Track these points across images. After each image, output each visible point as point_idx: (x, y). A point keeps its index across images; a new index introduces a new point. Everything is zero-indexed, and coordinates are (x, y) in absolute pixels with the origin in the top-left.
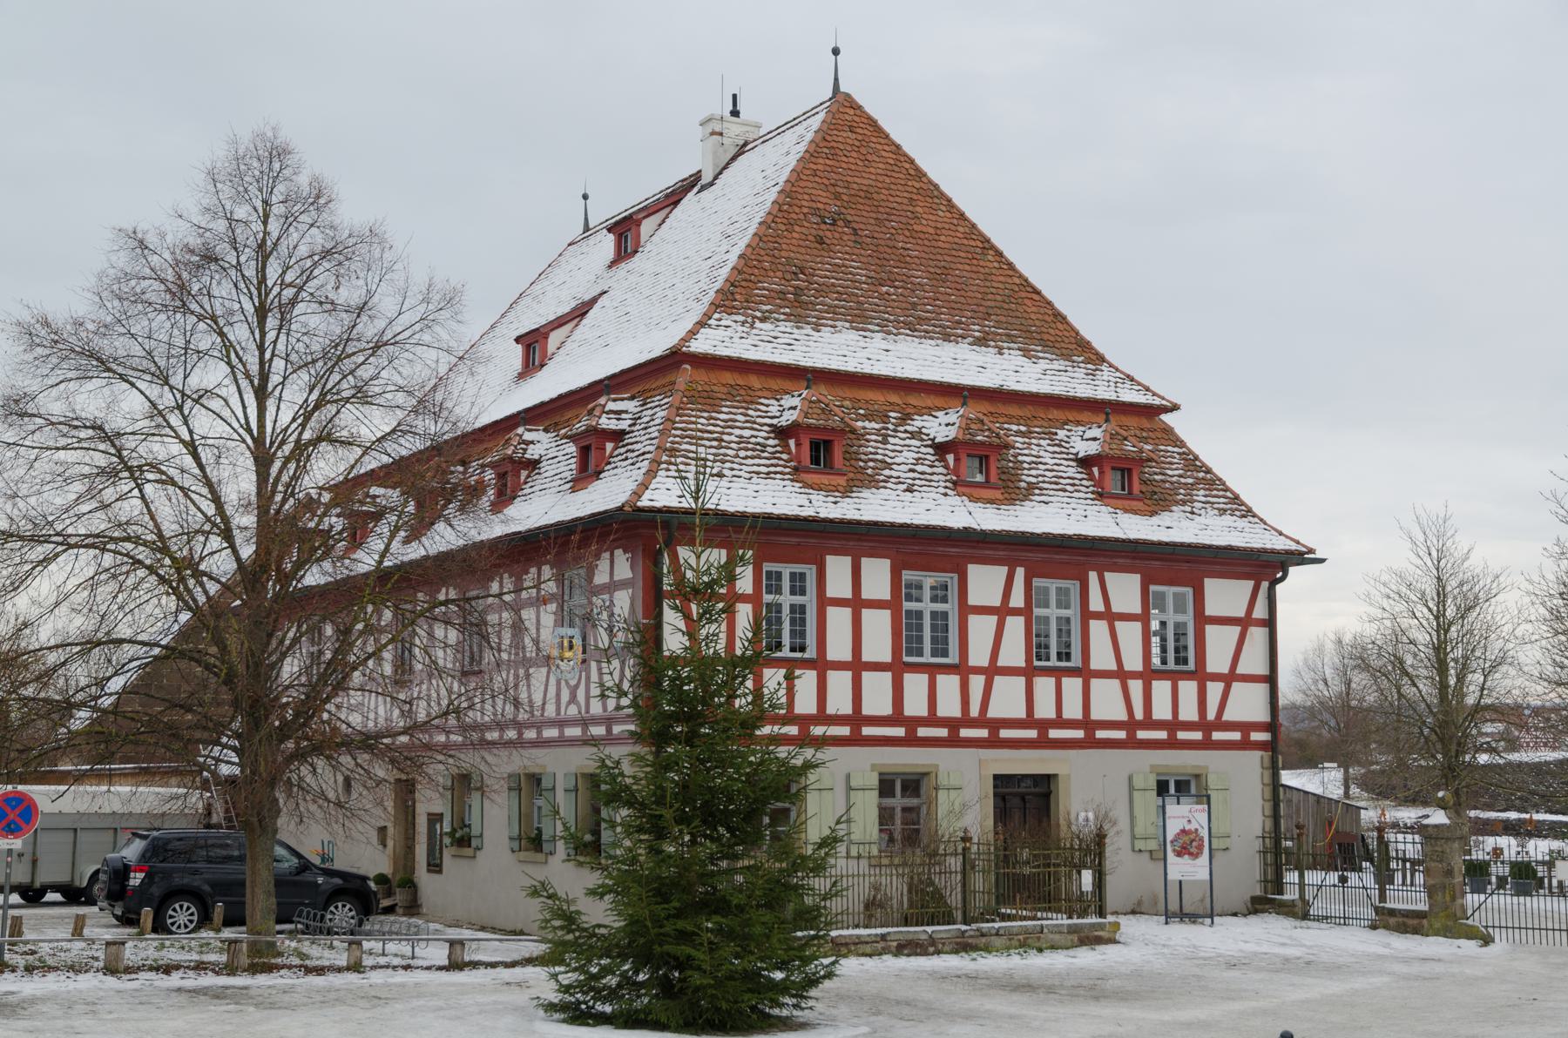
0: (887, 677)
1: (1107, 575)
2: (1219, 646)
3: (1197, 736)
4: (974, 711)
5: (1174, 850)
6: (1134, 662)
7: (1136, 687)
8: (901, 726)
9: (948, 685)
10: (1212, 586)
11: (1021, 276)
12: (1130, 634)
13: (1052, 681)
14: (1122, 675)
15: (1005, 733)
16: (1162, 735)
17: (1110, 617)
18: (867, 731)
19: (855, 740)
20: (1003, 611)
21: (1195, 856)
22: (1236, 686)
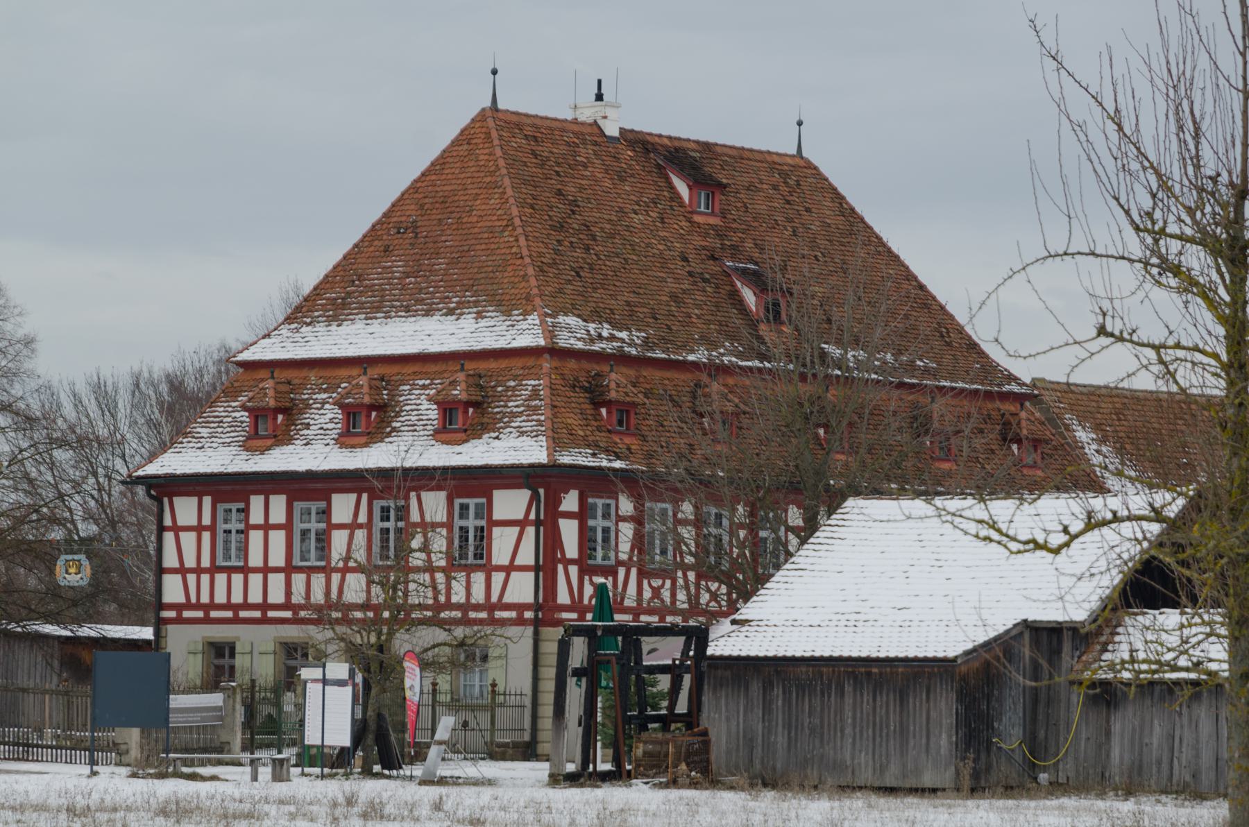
0: (282, 576)
3: (483, 615)
9: (318, 581)
10: (500, 497)
17: (266, 527)
18: (271, 614)
19: (264, 620)
20: (353, 527)
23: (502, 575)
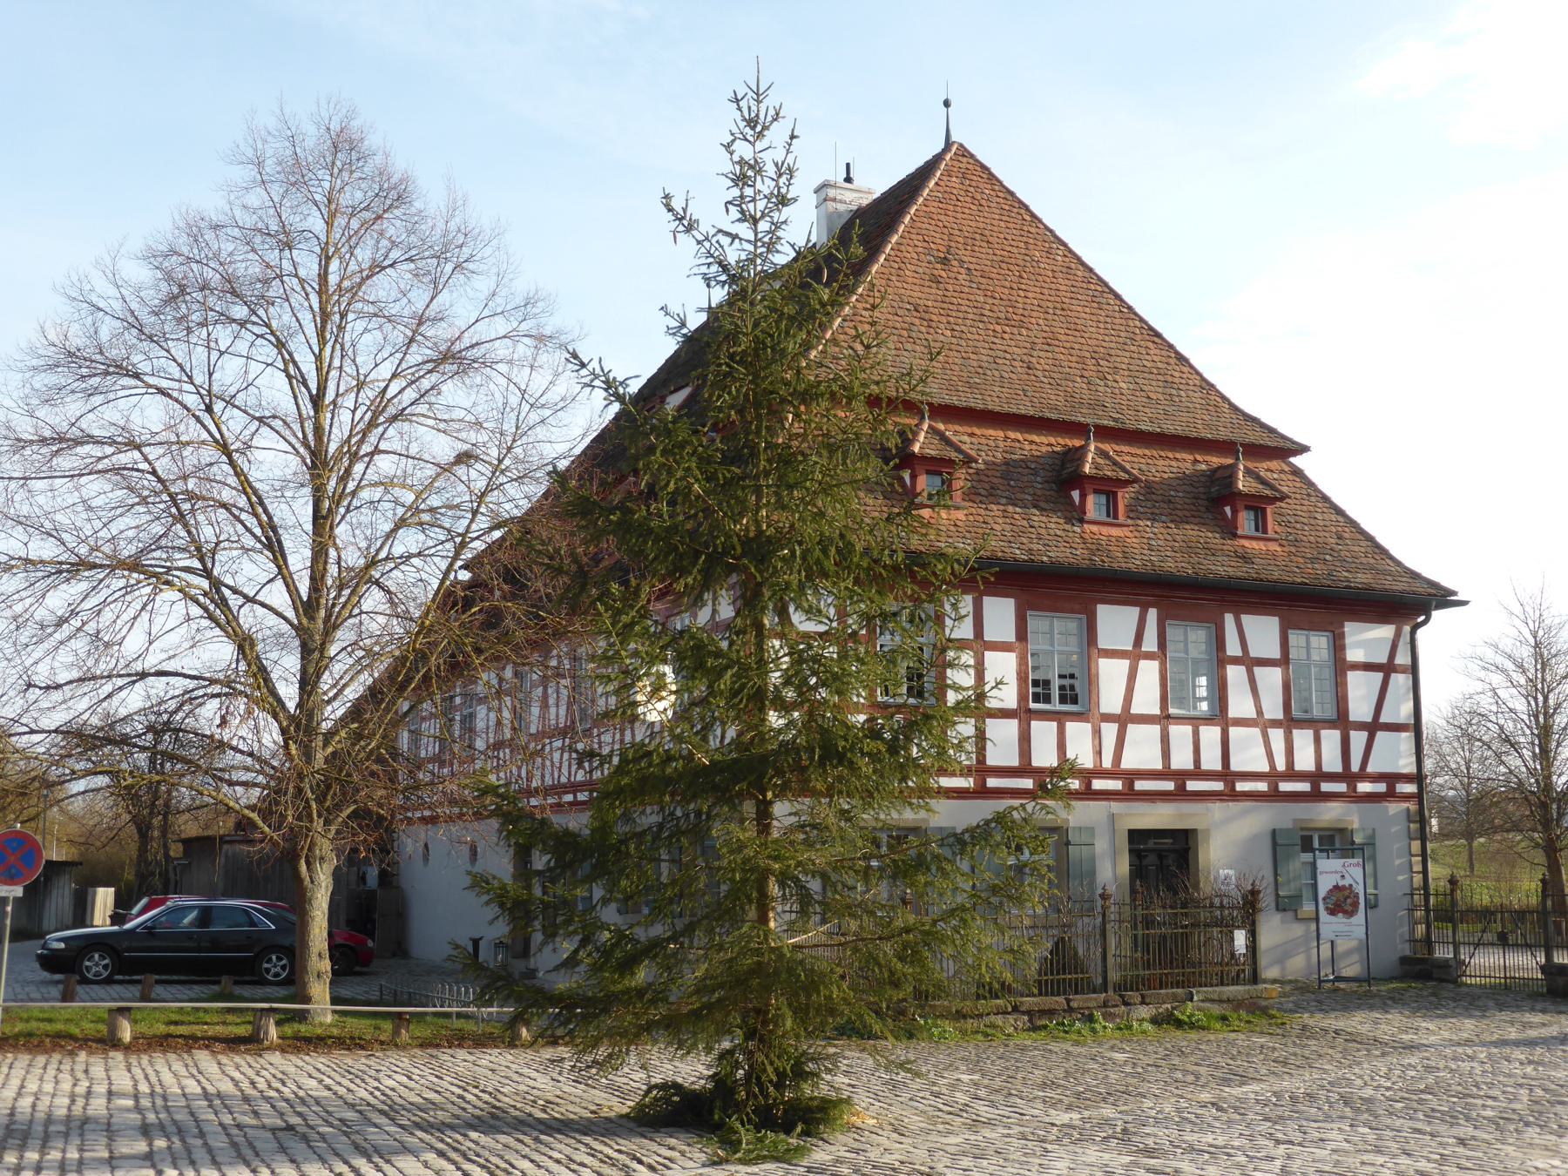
1: (1245, 618)
2: (1361, 694)
3: (1341, 787)
4: (1107, 763)
5: (1327, 909)
6: (1273, 710)
7: (1277, 736)
8: (1029, 777)
11: (1142, 320)
12: (1270, 678)
13: (1188, 729)
14: (1260, 722)
15: (1140, 785)
16: (1304, 787)
18: (992, 782)
21: (1350, 913)
22: (1380, 735)
23: (1364, 735)
